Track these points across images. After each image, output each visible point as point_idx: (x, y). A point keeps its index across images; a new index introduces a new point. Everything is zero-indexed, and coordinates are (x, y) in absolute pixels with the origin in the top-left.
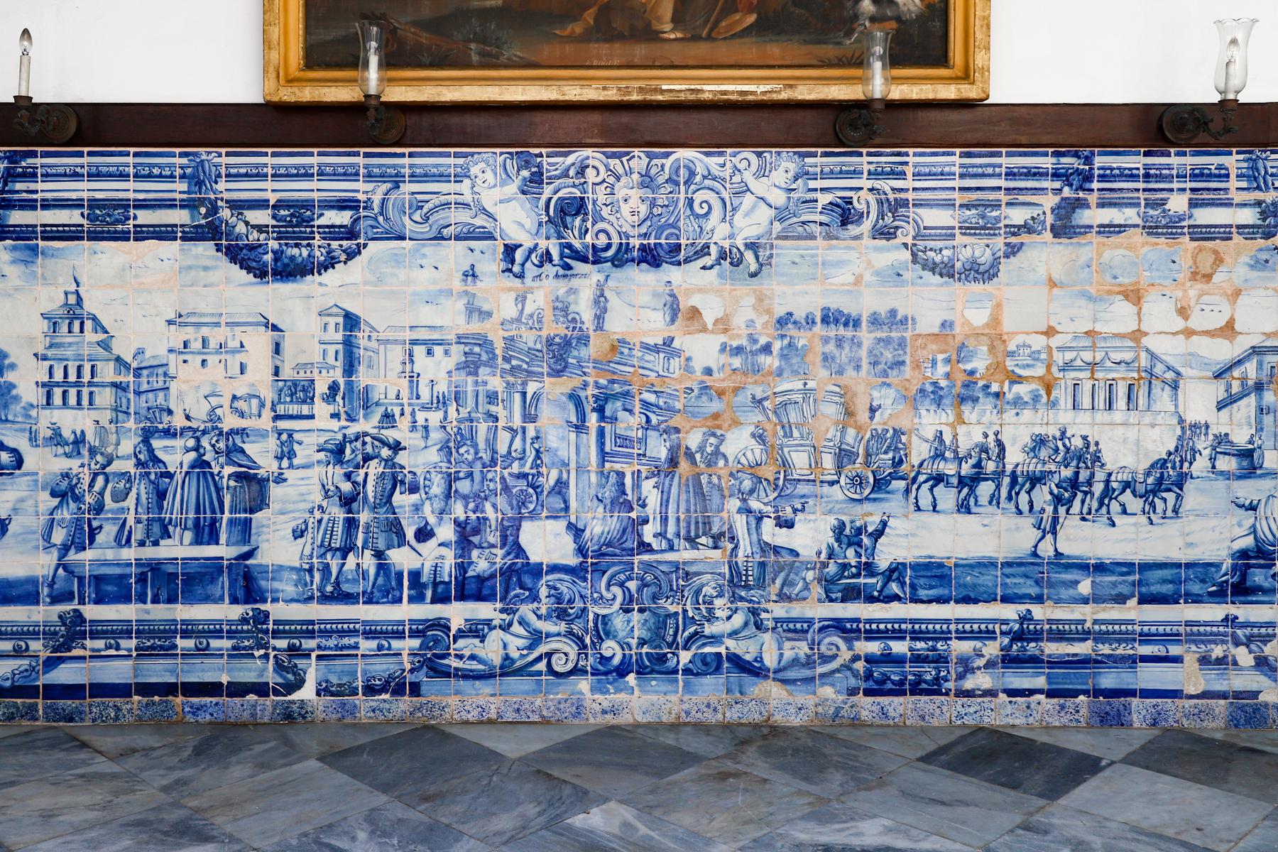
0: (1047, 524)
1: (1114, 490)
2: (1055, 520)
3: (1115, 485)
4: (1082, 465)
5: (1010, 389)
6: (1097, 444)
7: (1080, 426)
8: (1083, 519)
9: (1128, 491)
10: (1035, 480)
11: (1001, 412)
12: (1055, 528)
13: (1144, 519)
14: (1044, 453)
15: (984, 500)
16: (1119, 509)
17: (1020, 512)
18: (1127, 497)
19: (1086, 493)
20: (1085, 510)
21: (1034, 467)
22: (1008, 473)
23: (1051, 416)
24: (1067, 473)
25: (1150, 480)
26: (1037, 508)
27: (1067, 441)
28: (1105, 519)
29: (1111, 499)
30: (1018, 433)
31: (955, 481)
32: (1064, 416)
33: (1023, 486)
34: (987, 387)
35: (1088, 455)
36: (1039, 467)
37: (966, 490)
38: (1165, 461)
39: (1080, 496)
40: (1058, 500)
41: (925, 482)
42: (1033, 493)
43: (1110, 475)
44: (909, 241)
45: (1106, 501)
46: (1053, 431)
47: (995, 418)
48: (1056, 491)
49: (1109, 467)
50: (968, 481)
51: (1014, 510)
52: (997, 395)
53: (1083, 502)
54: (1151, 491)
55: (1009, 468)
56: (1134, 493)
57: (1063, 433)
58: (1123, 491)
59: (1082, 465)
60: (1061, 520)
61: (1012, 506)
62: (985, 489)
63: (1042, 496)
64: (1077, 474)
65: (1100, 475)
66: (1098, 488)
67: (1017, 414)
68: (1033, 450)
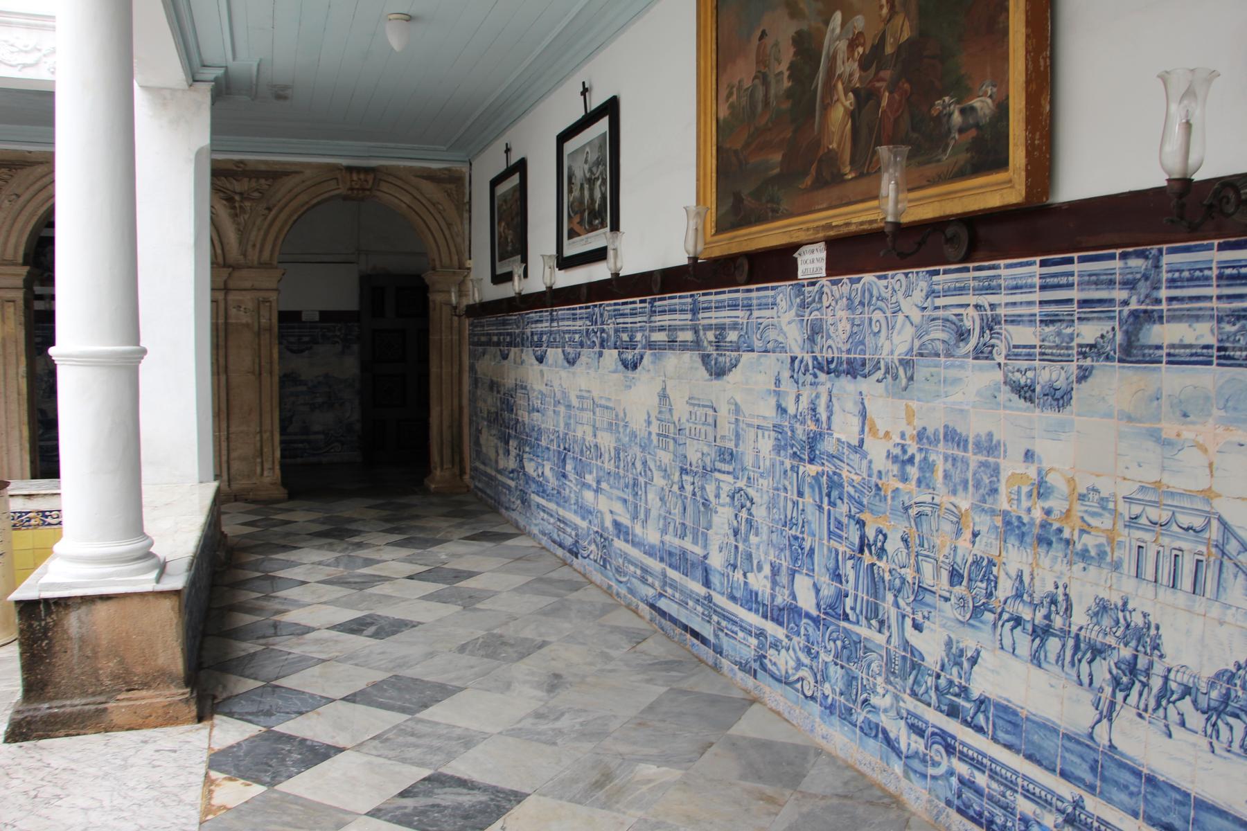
0: (1104, 706)
1: (1173, 692)
2: (1112, 704)
3: (1173, 686)
4: (1140, 648)
5: (1080, 537)
6: (1157, 628)
7: (1146, 602)
8: (1140, 715)
9: (1188, 698)
10: (1097, 651)
11: (1070, 563)
12: (1111, 715)
13: (1204, 742)
14: (1106, 622)
15: (1052, 657)
16: (1177, 718)
17: (1081, 684)
18: (1186, 705)
19: (1144, 685)
20: (1142, 706)
21: (1094, 635)
22: (1072, 635)
23: (1114, 580)
24: (1126, 653)
25: (1214, 694)
26: (1096, 684)
27: (1128, 614)
28: (1161, 724)
29: (1169, 702)
30: (1087, 587)
31: (1029, 627)
32: (1128, 585)
33: (1085, 654)
34: (1060, 531)
35: (1145, 638)
36: (1100, 638)
37: (1037, 641)
38: (1233, 675)
39: (1137, 686)
40: (1116, 682)
41: (1008, 621)
42: (1094, 664)
43: (1169, 670)
44: (1002, 360)
45: (1164, 703)
46: (1116, 599)
47: (1065, 568)
48: (1115, 671)
49: (1168, 661)
50: (1040, 632)
51: (1075, 678)
52: (1068, 542)
53: (1141, 695)
54: (1215, 709)
55: (1074, 629)
56: (1195, 702)
57: (1125, 604)
58: (1182, 698)
59: (1140, 648)
60: (1118, 707)
61: (1073, 672)
62: (1053, 644)
63: (1102, 670)
64: (1136, 657)
65: (1158, 669)
66: (1156, 683)
67: (1085, 569)
68: (1096, 614)
